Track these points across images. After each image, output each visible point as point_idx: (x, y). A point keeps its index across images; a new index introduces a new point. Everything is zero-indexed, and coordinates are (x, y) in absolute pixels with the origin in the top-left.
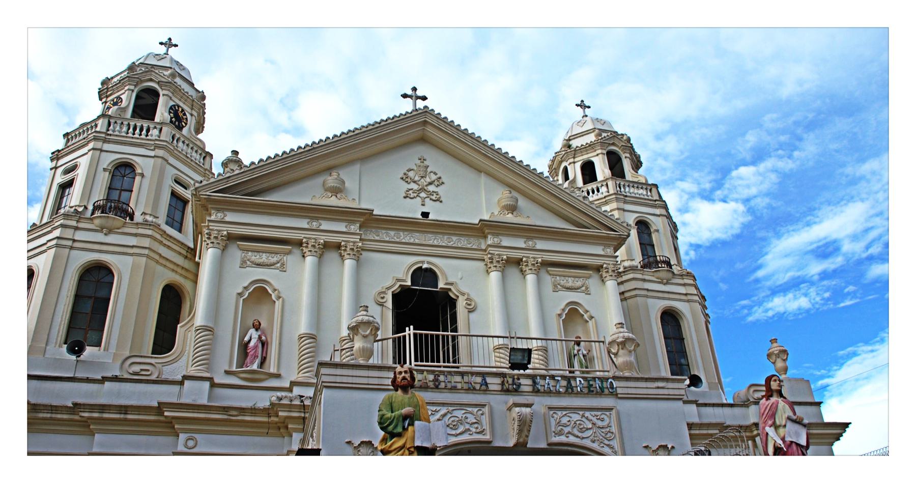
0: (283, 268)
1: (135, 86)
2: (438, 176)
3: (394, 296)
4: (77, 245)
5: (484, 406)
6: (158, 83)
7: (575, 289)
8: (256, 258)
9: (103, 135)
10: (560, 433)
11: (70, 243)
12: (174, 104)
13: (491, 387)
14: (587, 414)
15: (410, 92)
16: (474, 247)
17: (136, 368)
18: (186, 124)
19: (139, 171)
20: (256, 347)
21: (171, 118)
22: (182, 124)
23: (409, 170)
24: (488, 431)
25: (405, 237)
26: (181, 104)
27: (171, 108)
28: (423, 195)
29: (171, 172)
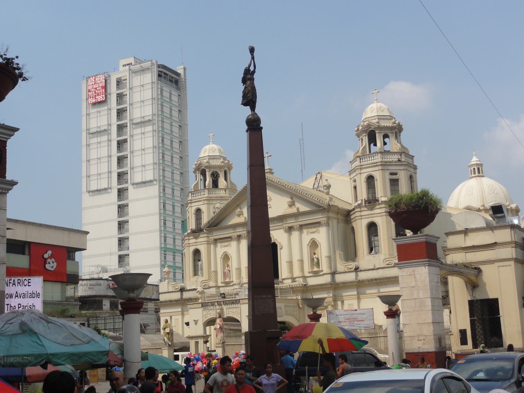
0: (230, 246)
1: (198, 171)
2: (270, 197)
4: (190, 245)
7: (314, 232)
8: (224, 244)
10: (229, 314)
11: (188, 245)
12: (211, 172)
14: (234, 309)
17: (204, 284)
18: (219, 177)
19: (202, 211)
21: (212, 179)
22: (218, 178)
24: (215, 315)
26: (215, 170)
27: (211, 175)
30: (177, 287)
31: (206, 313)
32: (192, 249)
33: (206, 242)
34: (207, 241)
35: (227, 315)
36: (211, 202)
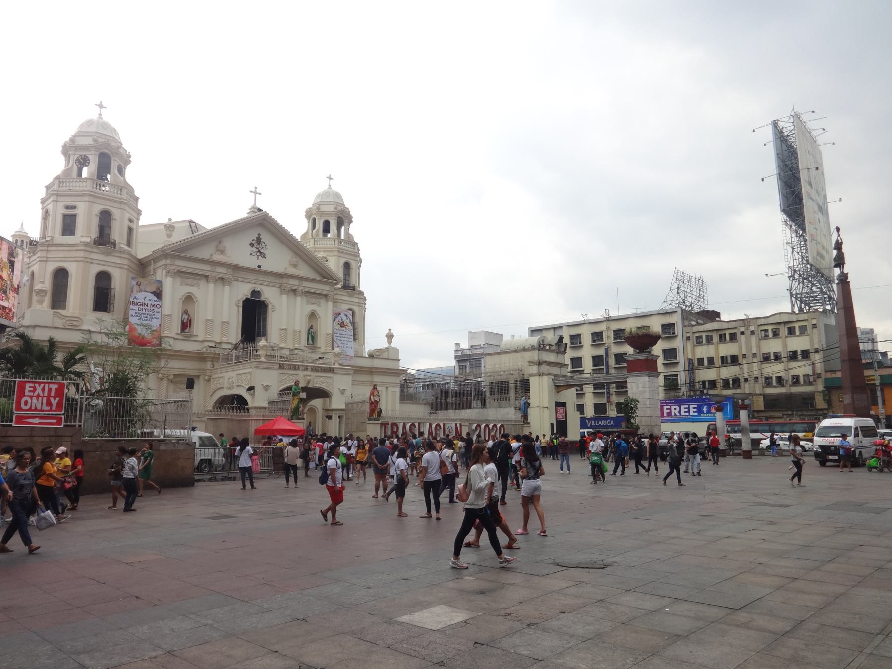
0: (198, 287)
3: (244, 302)
5: (298, 374)
6: (111, 152)
9: (93, 194)
10: (316, 383)
11: (89, 260)
13: (301, 369)
15: (253, 190)
16: (277, 282)
20: (187, 321)
23: (253, 240)
25: (250, 276)
28: (258, 254)
29: (127, 216)
30: (75, 323)
31: (284, 378)
32: (95, 269)
33: (127, 267)
34: (128, 265)
35: (316, 385)
36: (60, 198)
